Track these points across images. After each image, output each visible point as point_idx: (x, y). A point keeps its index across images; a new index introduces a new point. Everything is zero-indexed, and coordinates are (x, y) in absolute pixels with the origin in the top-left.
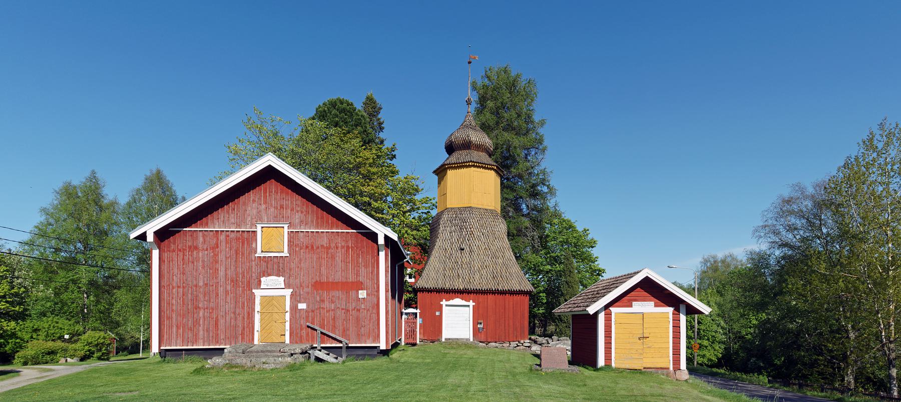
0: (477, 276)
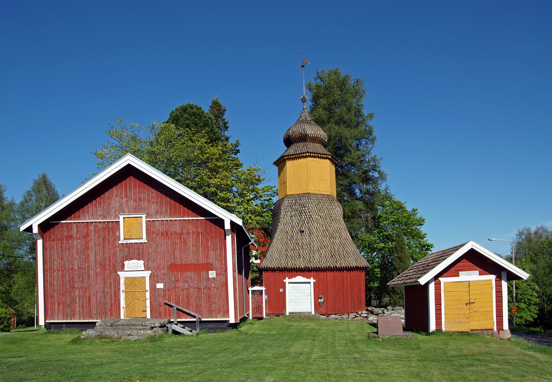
0: (317, 256)
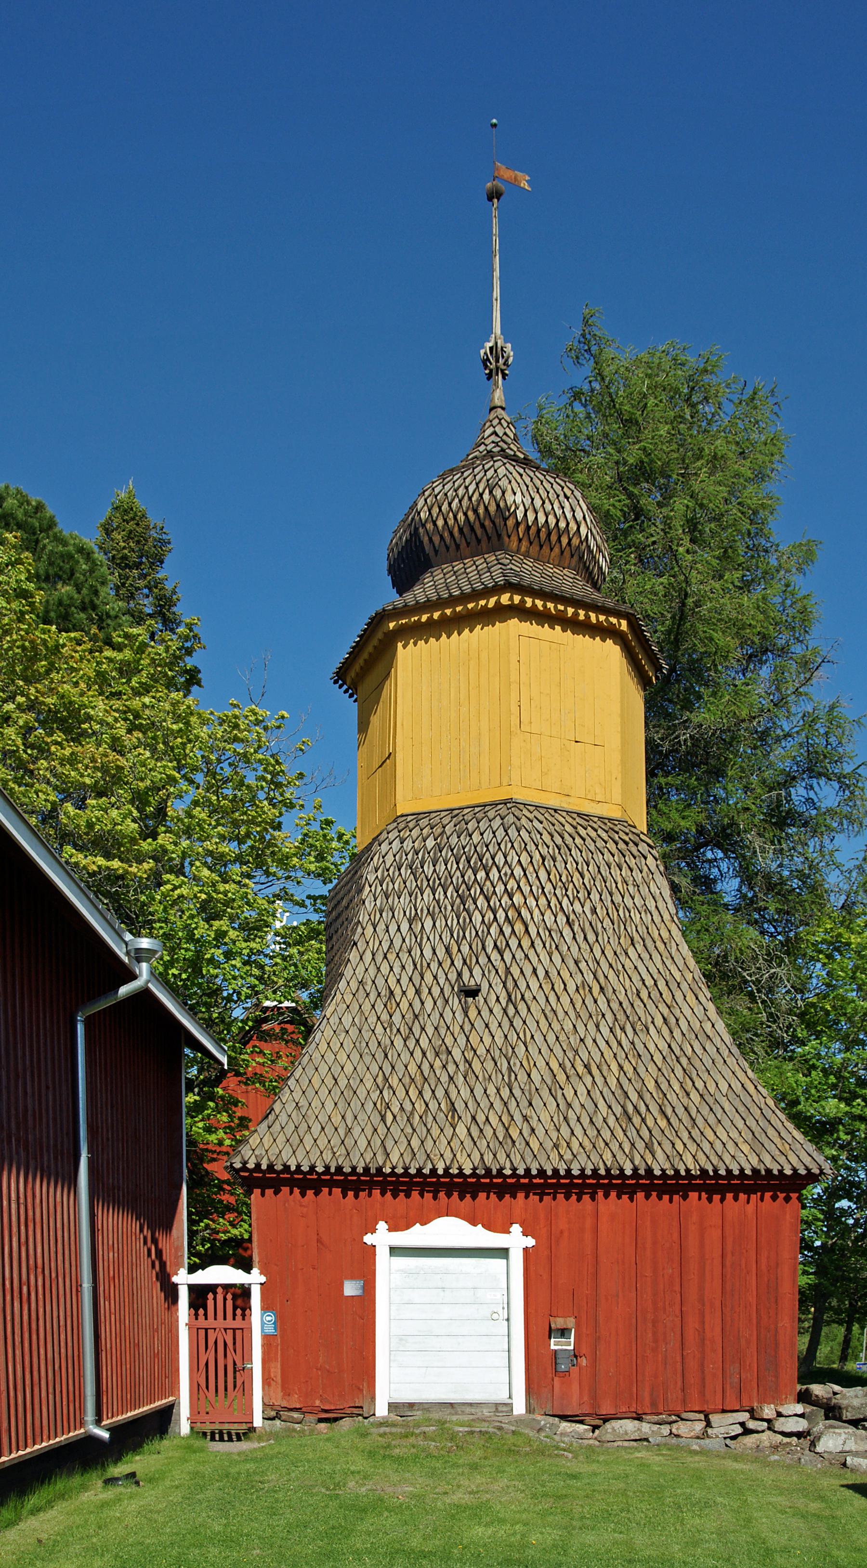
0: (545, 1113)
